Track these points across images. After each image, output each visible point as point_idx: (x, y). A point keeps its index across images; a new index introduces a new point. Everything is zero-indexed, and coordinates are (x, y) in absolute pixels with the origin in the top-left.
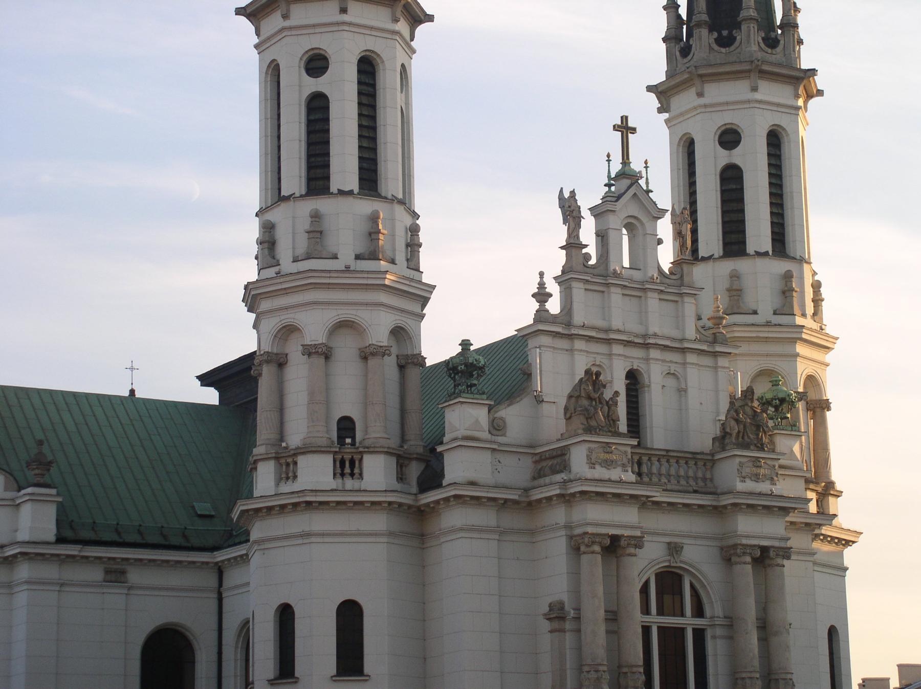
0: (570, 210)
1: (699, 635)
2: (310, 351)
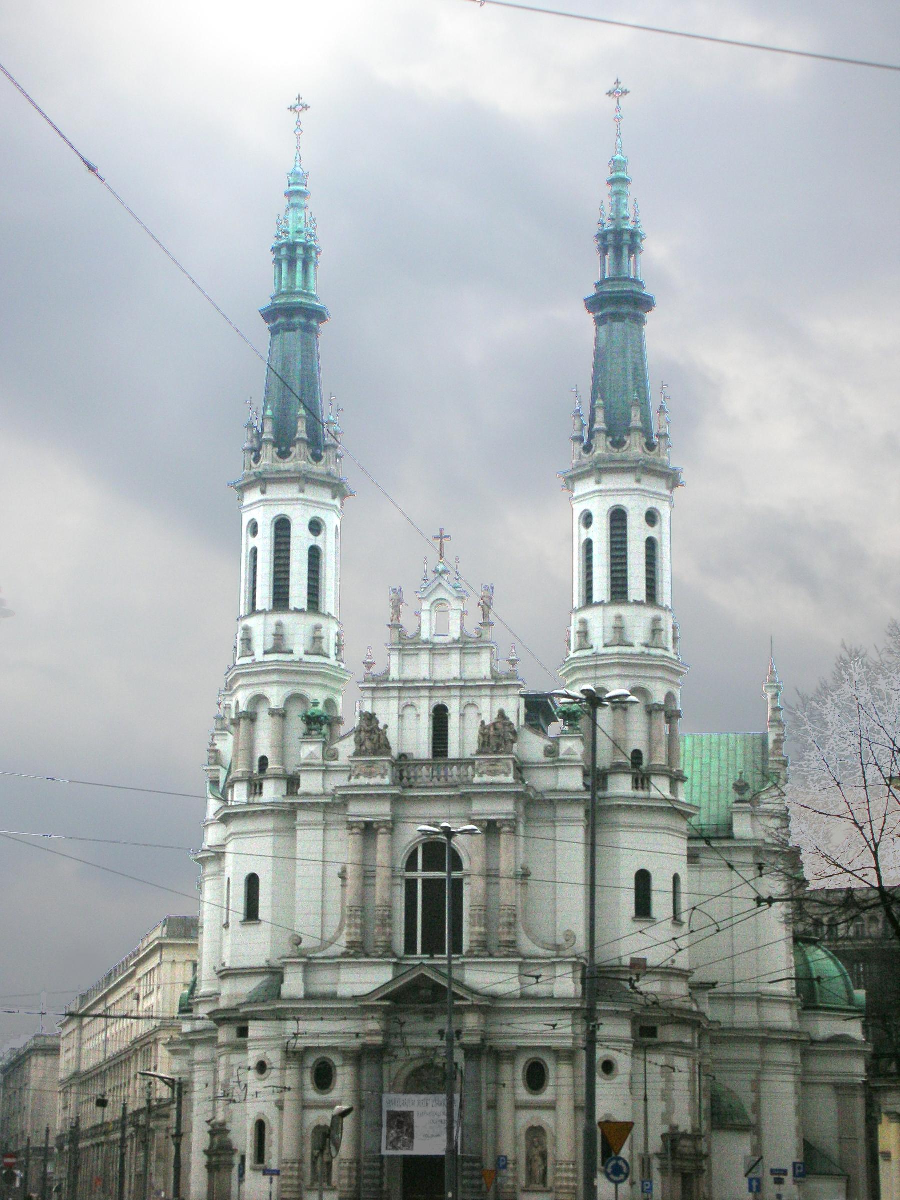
1: (457, 885)
2: (273, 713)
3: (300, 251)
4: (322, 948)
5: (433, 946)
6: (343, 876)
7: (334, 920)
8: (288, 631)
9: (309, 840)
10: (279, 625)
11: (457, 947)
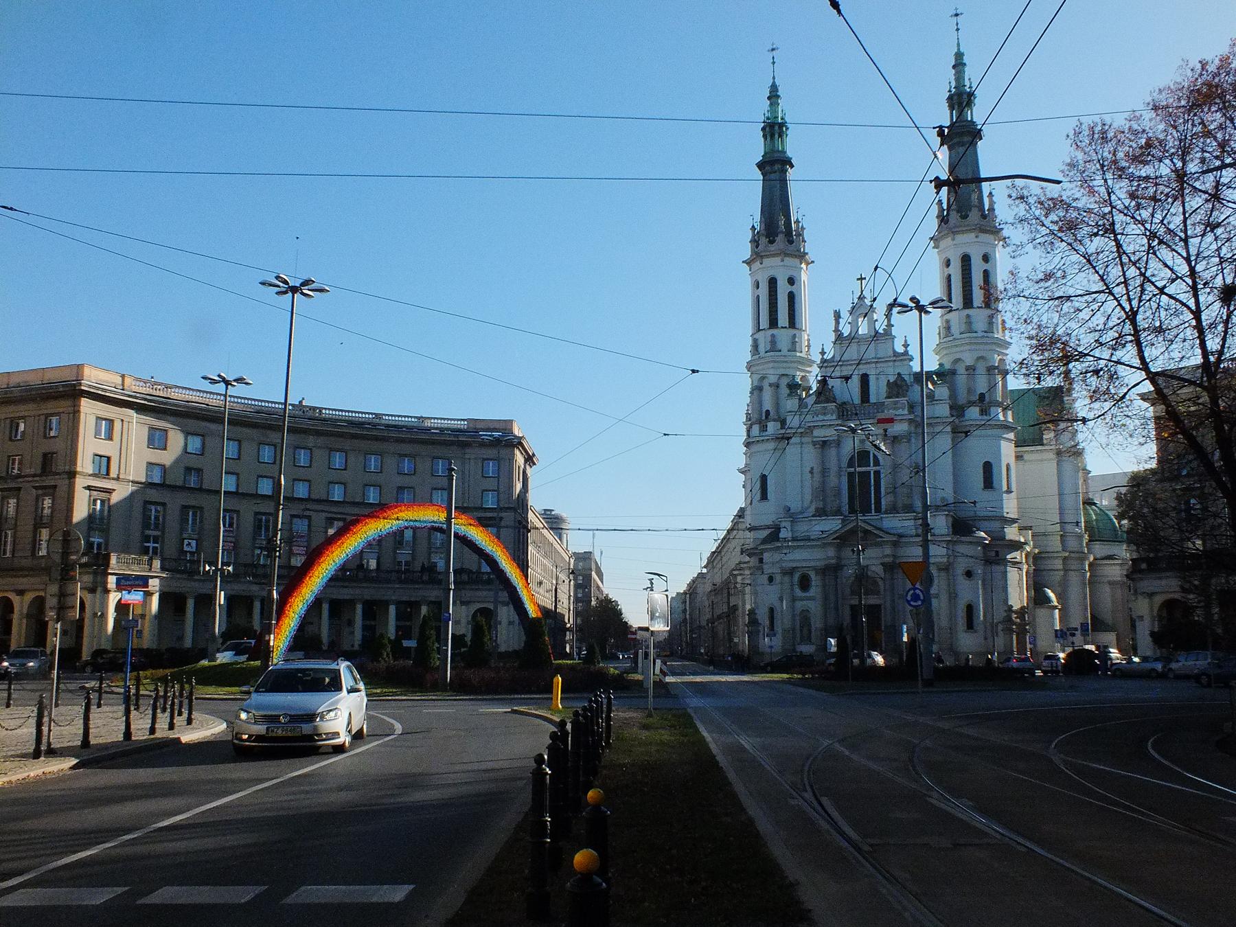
0: (837, 316)
1: (877, 473)
2: (770, 385)
3: (777, 128)
4: (801, 513)
5: (866, 510)
6: (811, 472)
7: (808, 497)
8: (778, 339)
9: (792, 451)
11: (878, 510)
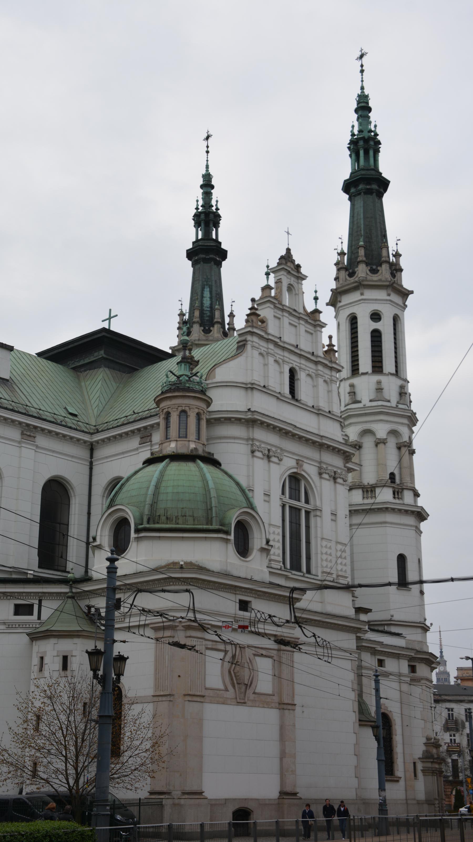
10: (379, 383)
